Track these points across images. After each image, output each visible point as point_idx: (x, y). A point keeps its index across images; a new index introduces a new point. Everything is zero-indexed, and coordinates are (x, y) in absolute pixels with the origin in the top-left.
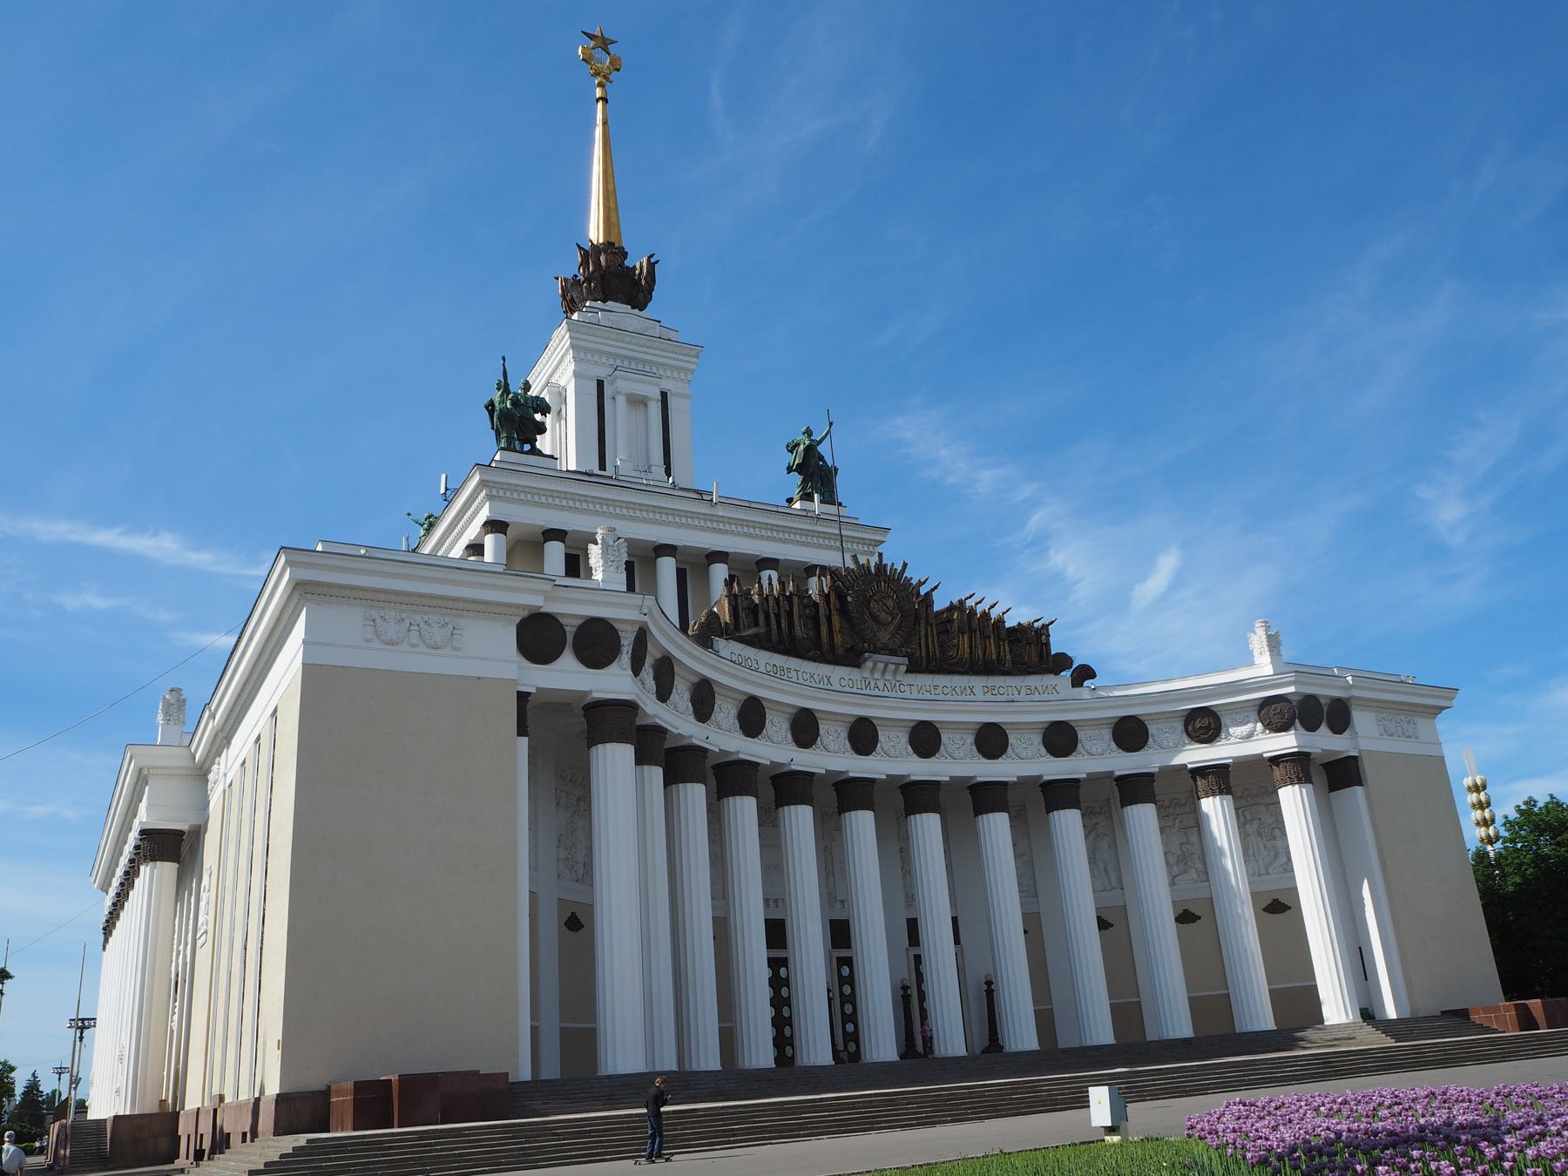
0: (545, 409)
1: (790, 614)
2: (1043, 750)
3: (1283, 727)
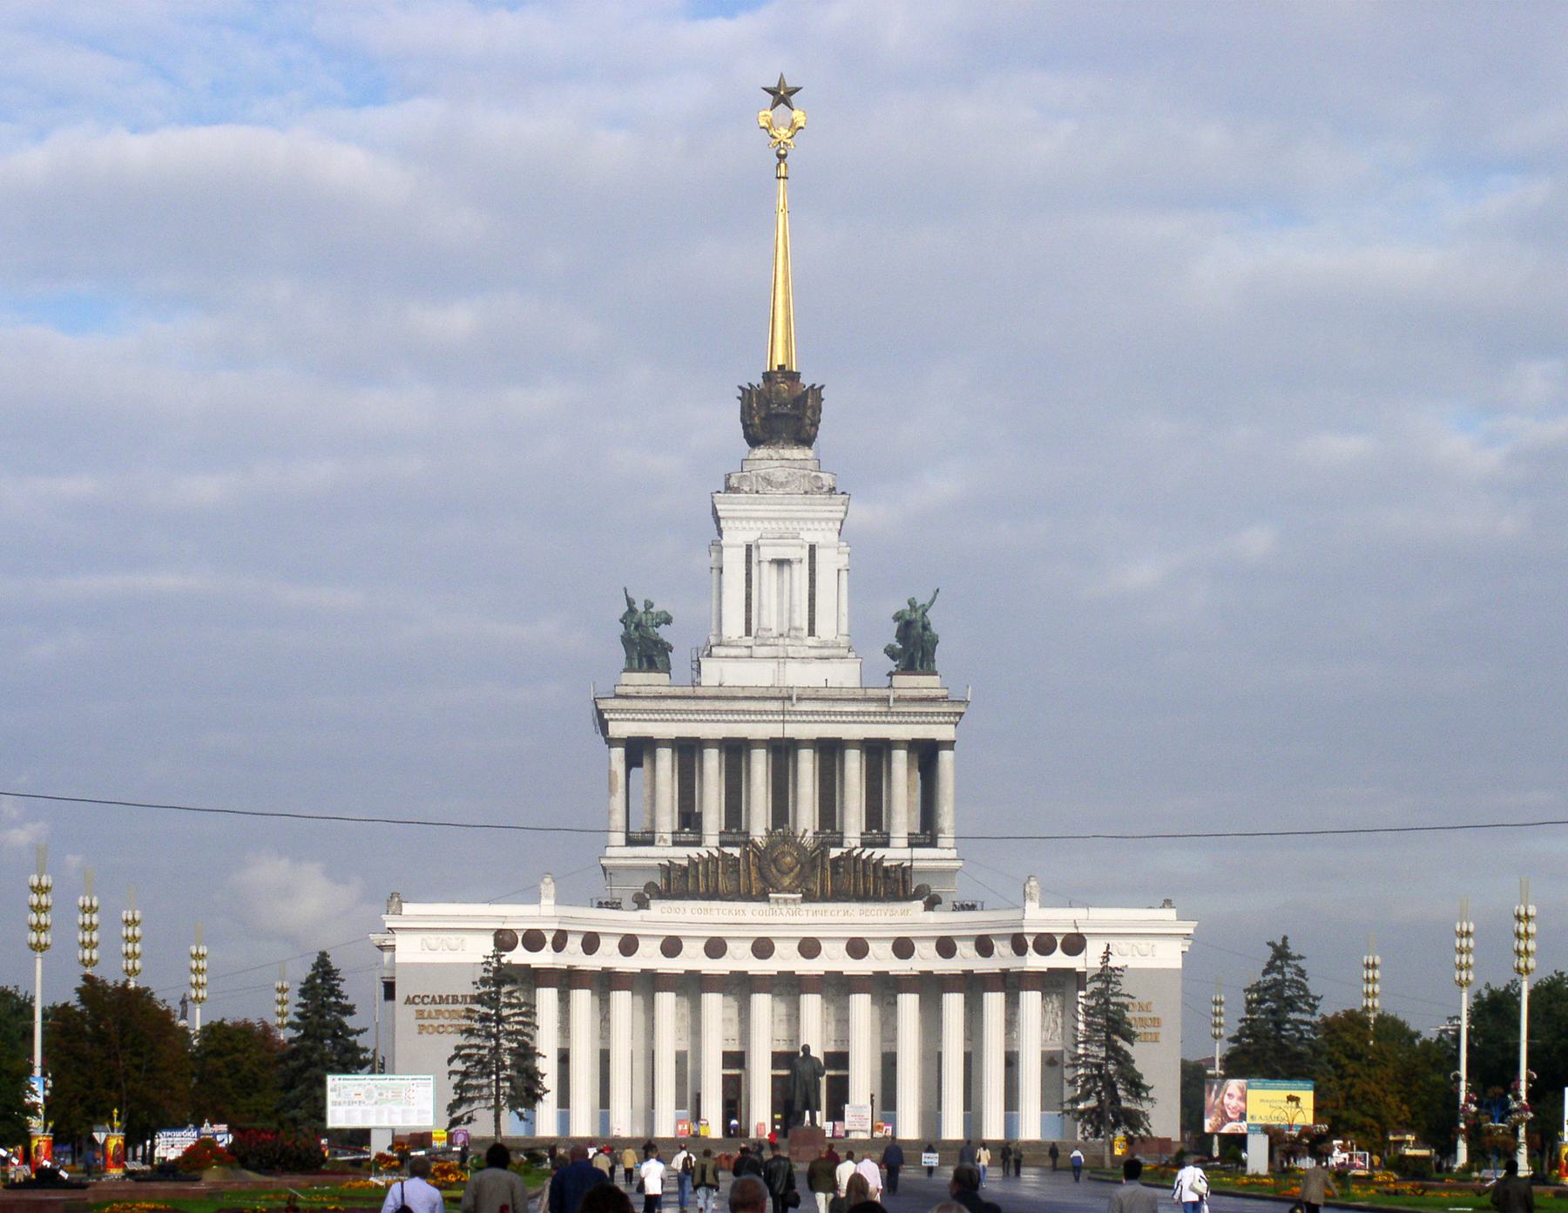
0: (668, 621)
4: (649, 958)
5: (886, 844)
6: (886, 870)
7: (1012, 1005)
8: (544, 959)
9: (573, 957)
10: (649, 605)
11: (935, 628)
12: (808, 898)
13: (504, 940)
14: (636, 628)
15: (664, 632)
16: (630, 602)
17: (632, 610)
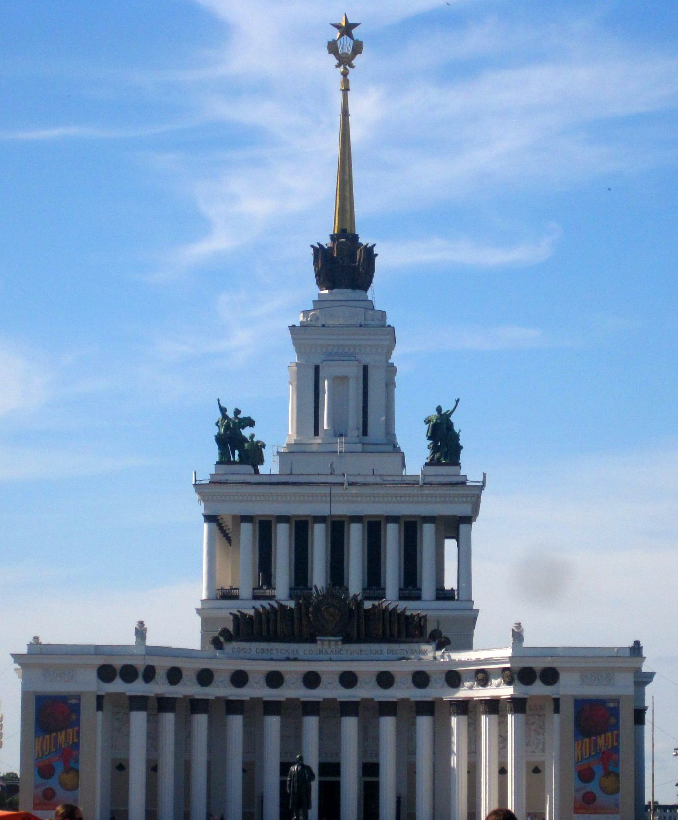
0: (250, 422)
1: (276, 621)
2: (412, 685)
3: (509, 683)
4: (221, 689)
5: (418, 598)
6: (407, 617)
7: (502, 725)
8: (138, 688)
9: (160, 688)
10: (237, 412)
11: (456, 428)
12: (347, 640)
13: (106, 673)
14: (226, 430)
15: (246, 432)
16: (223, 410)
17: (225, 416)
